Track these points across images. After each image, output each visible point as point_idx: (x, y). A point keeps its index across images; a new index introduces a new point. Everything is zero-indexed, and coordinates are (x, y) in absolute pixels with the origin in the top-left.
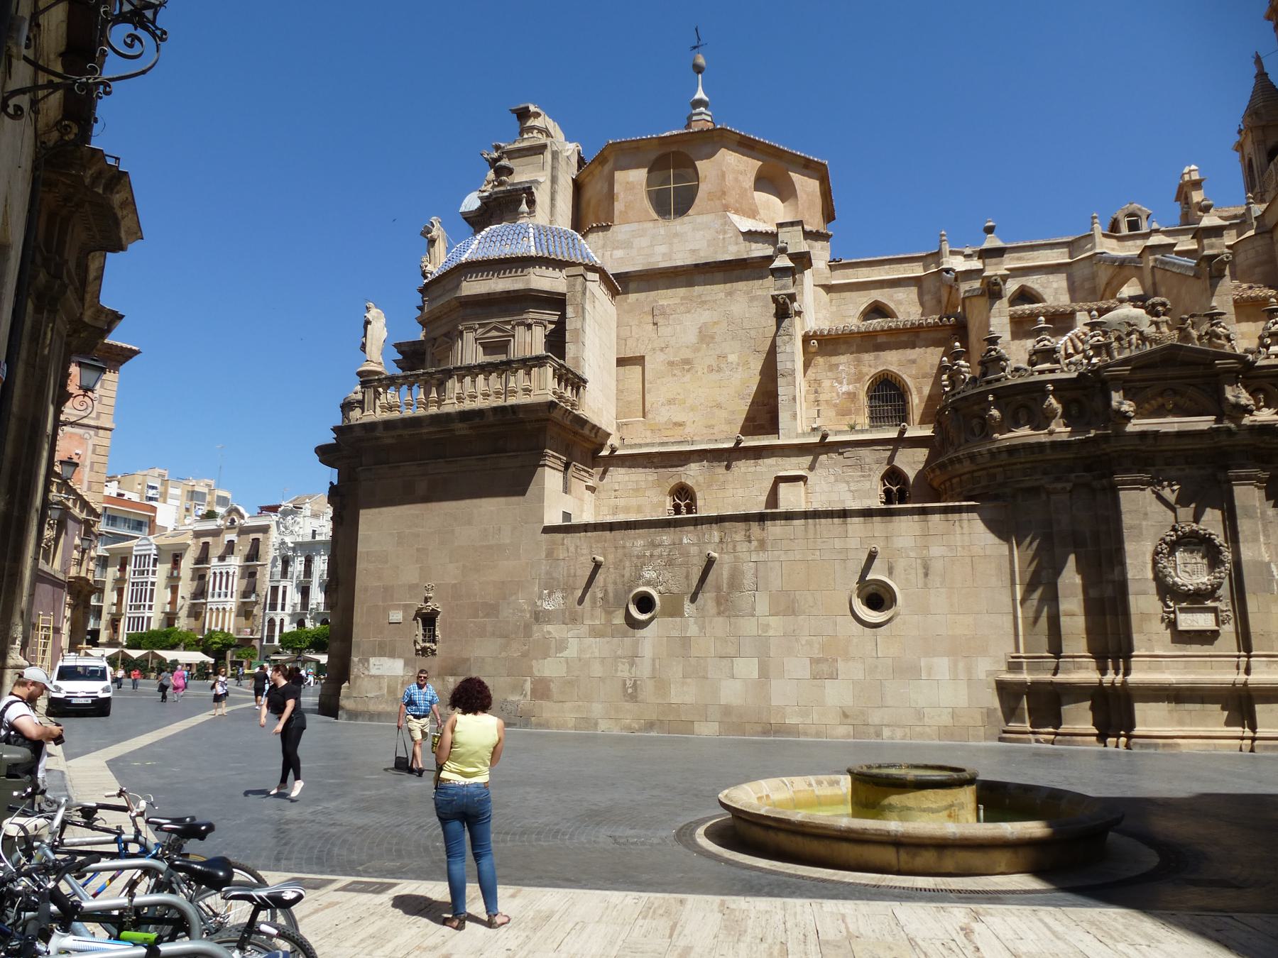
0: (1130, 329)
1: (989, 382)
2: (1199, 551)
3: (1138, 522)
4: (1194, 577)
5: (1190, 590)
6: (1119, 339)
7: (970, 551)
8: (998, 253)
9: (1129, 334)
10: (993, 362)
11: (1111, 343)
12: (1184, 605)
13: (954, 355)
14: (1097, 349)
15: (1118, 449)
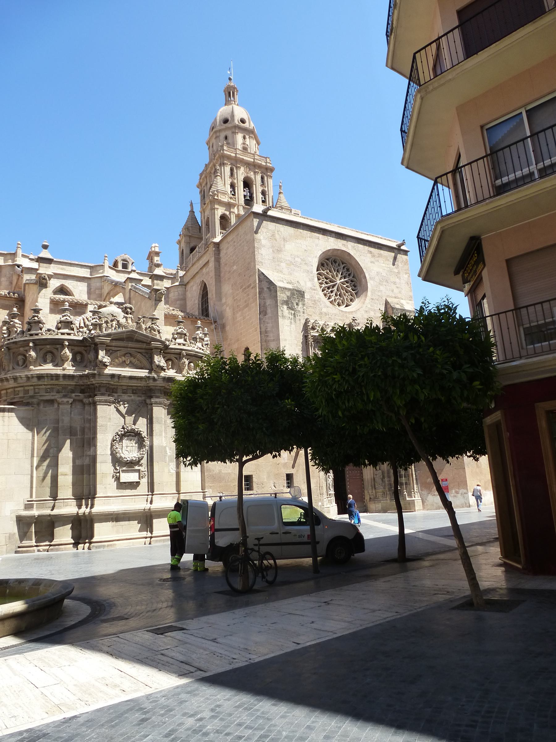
0: (113, 318)
1: (31, 335)
2: (134, 440)
3: (106, 423)
4: (131, 453)
5: (128, 460)
6: (107, 322)
7: (7, 436)
8: (49, 261)
9: (112, 321)
10: (35, 324)
11: (102, 324)
12: (124, 468)
13: (12, 315)
14: (95, 325)
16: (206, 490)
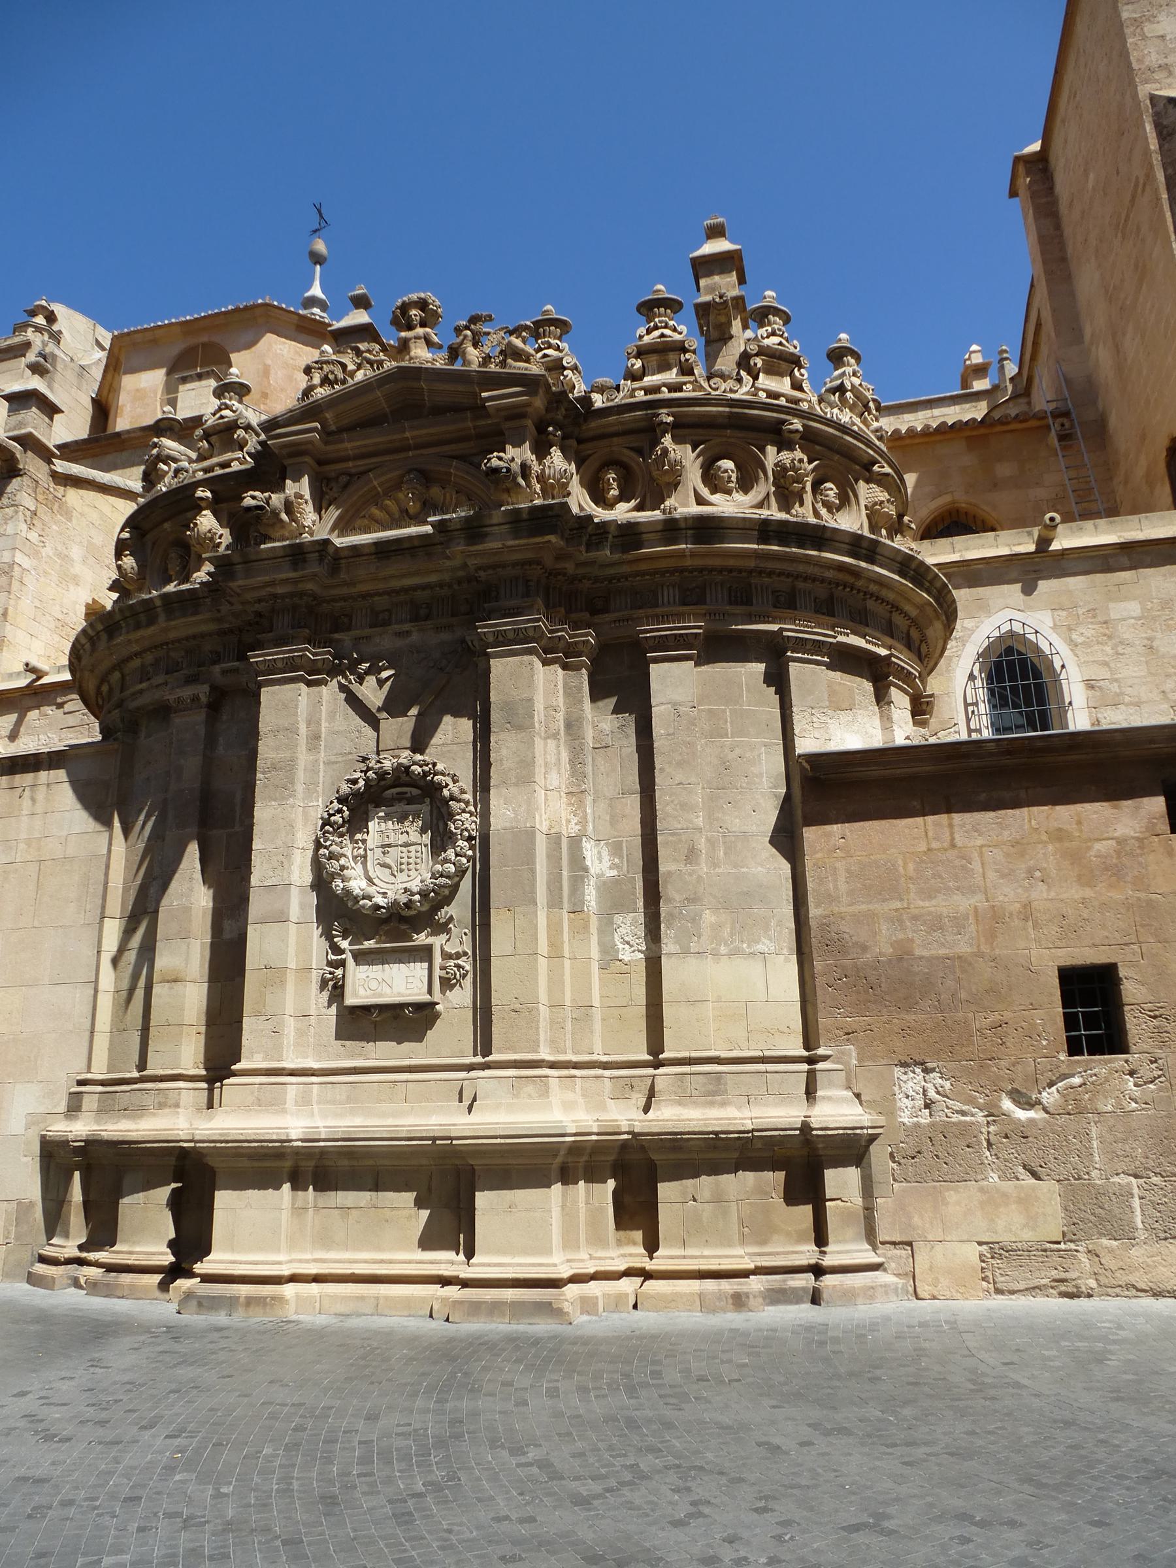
2: (416, 816)
5: (378, 907)
12: (369, 944)
15: (263, 593)
16: (821, 1051)
